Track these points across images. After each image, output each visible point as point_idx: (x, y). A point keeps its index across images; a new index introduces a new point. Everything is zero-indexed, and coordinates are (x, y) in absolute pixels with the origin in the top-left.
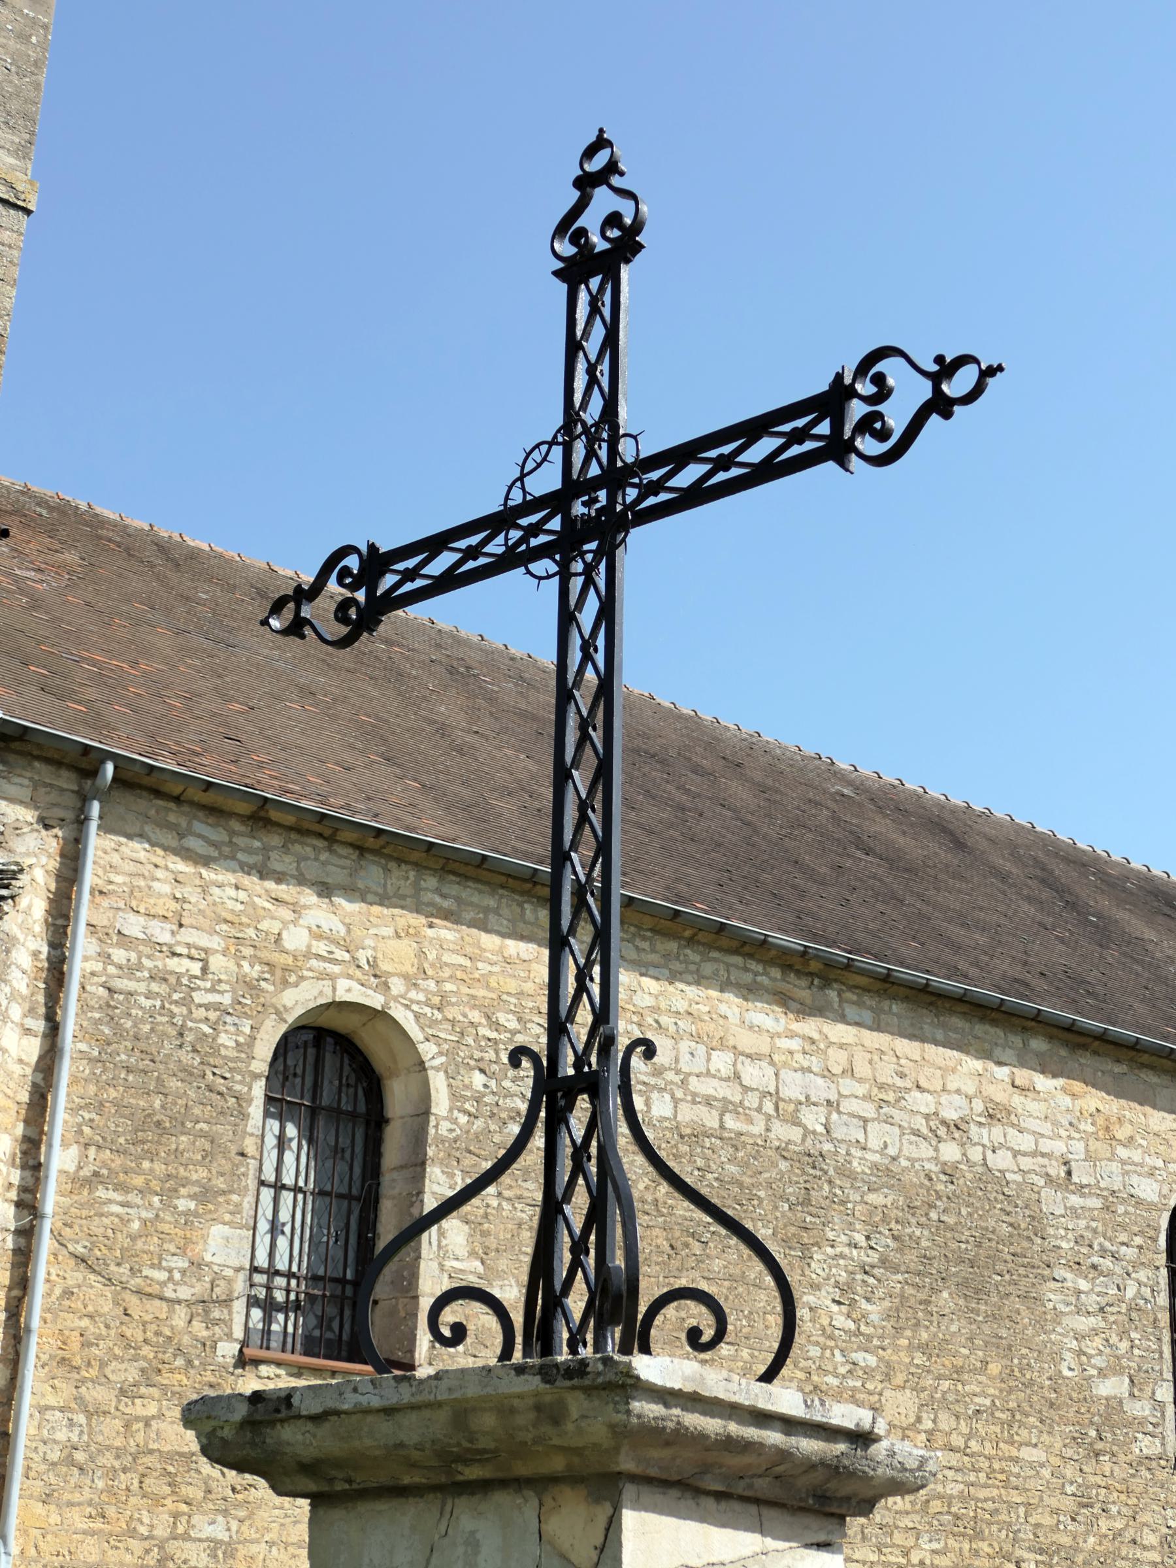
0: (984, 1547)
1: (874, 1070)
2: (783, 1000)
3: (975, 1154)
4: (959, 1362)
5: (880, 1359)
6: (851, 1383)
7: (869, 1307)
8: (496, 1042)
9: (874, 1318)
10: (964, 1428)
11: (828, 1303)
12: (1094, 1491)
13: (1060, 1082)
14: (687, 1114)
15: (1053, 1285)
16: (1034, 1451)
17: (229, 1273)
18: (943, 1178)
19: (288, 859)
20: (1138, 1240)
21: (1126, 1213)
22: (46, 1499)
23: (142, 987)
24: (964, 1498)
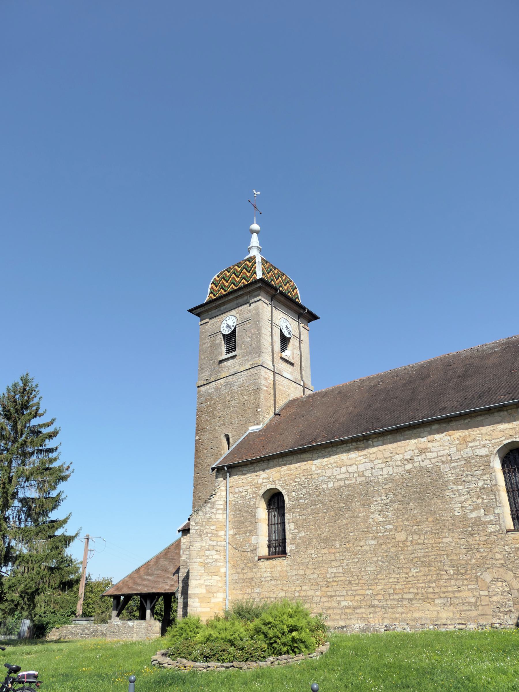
0: (433, 568)
1: (383, 455)
2: (357, 449)
3: (417, 464)
4: (418, 520)
5: (394, 526)
6: (386, 534)
7: (388, 514)
8: (295, 485)
9: (390, 516)
10: (422, 537)
11: (377, 516)
12: (473, 546)
13: (445, 433)
14: (336, 484)
15: (449, 491)
16: (448, 539)
17: (256, 544)
18: (407, 474)
19: (257, 467)
20: (482, 468)
21: (476, 461)
22: (234, 589)
23: (239, 500)
24: (424, 556)
